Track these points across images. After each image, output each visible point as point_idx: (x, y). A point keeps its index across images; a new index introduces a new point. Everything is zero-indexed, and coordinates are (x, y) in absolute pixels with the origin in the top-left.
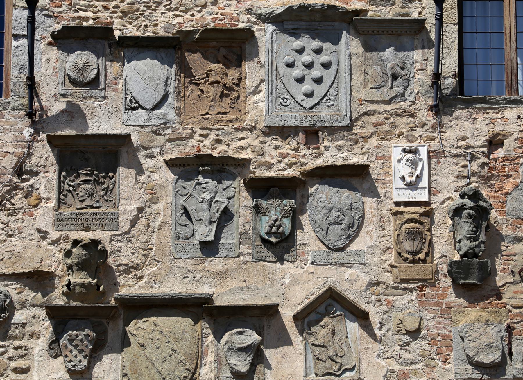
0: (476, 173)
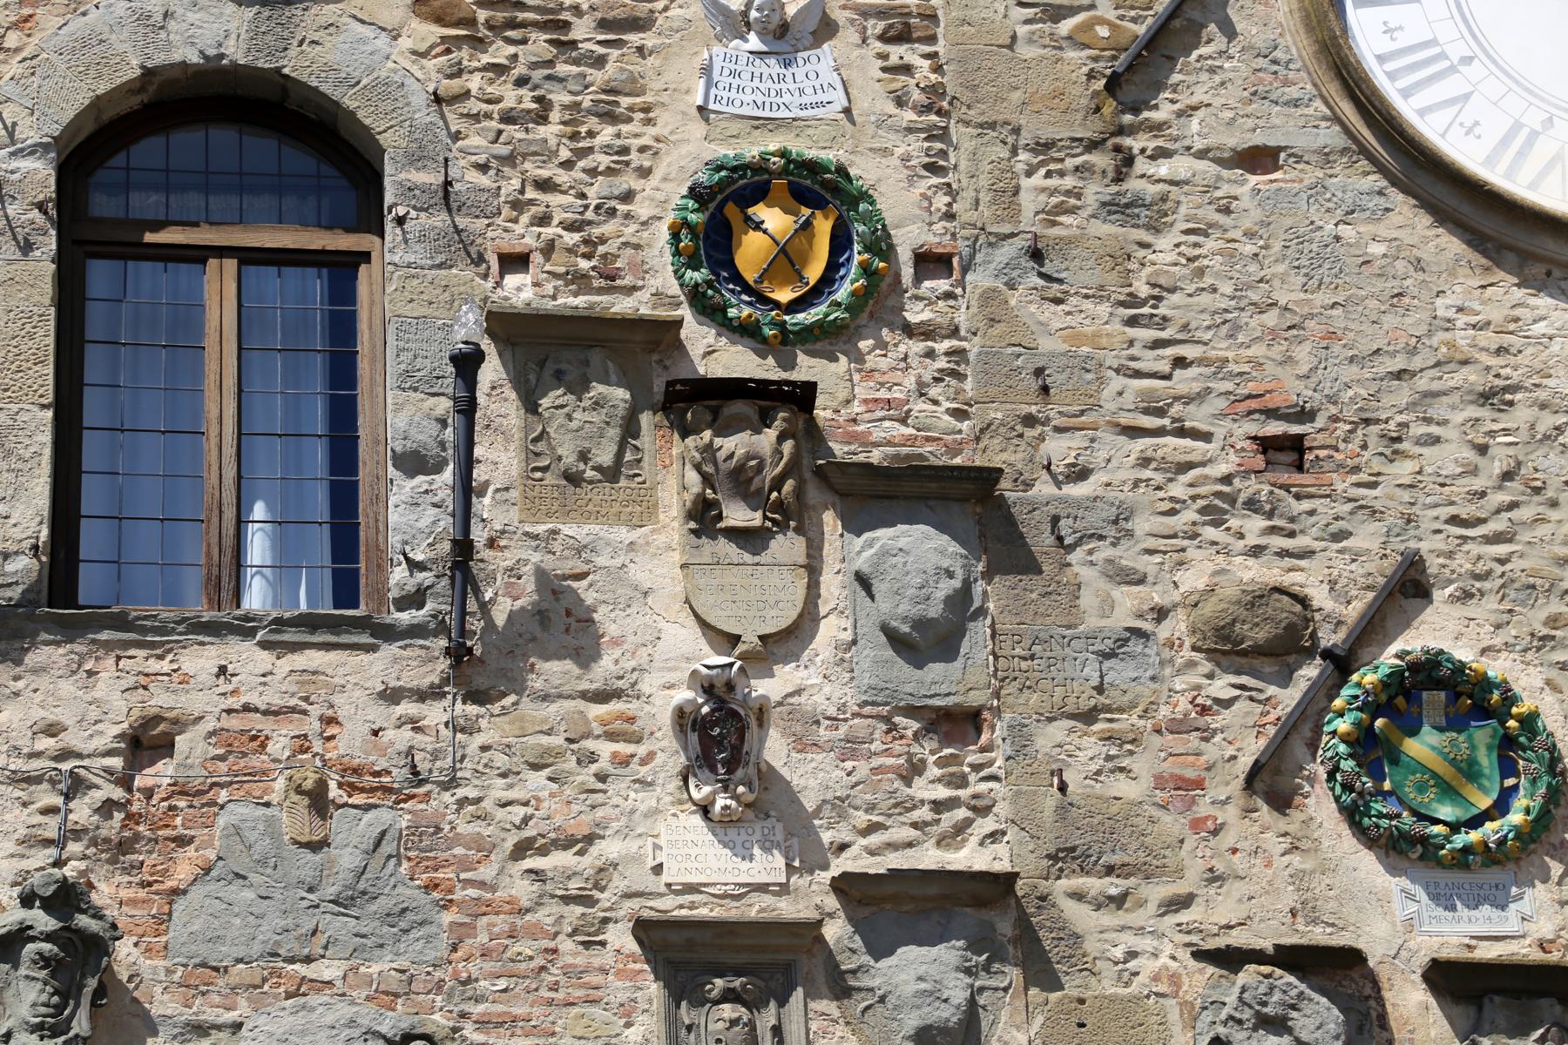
0: (85, 831)
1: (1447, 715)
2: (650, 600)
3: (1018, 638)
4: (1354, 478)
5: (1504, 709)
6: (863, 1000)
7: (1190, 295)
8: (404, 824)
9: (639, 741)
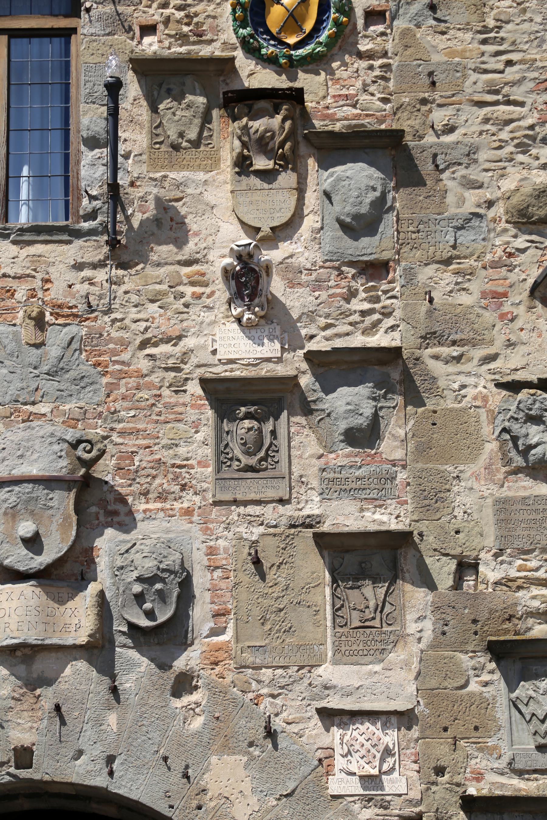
2: (214, 211)
3: (411, 221)
6: (319, 415)
7: (518, 24)
8: (84, 333)
9: (207, 285)
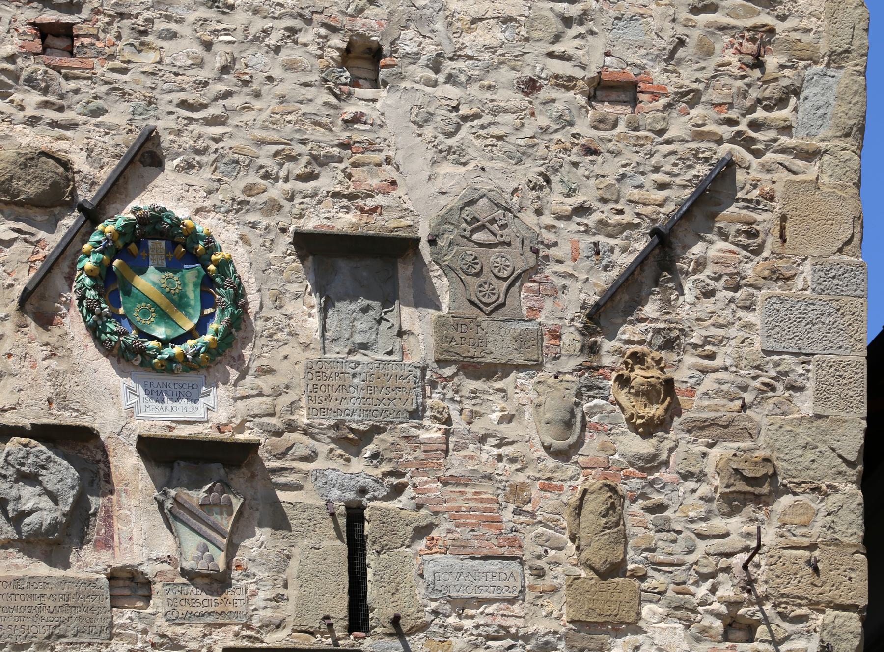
1: (167, 259)
4: (111, 64)
5: (207, 256)
